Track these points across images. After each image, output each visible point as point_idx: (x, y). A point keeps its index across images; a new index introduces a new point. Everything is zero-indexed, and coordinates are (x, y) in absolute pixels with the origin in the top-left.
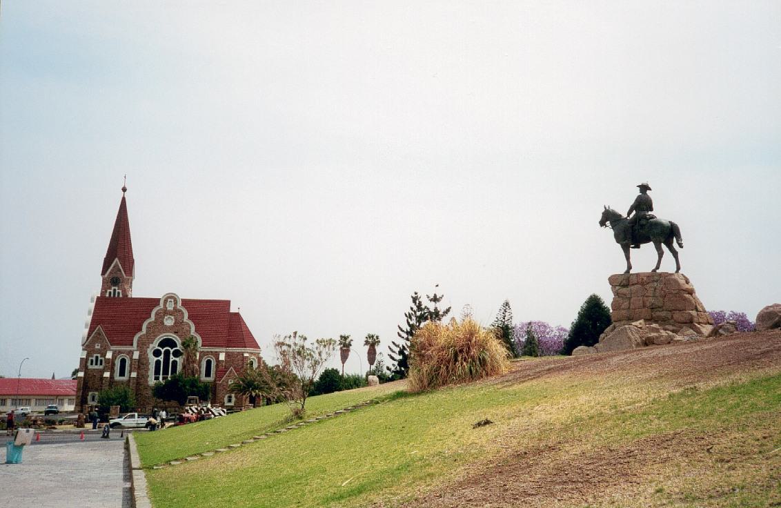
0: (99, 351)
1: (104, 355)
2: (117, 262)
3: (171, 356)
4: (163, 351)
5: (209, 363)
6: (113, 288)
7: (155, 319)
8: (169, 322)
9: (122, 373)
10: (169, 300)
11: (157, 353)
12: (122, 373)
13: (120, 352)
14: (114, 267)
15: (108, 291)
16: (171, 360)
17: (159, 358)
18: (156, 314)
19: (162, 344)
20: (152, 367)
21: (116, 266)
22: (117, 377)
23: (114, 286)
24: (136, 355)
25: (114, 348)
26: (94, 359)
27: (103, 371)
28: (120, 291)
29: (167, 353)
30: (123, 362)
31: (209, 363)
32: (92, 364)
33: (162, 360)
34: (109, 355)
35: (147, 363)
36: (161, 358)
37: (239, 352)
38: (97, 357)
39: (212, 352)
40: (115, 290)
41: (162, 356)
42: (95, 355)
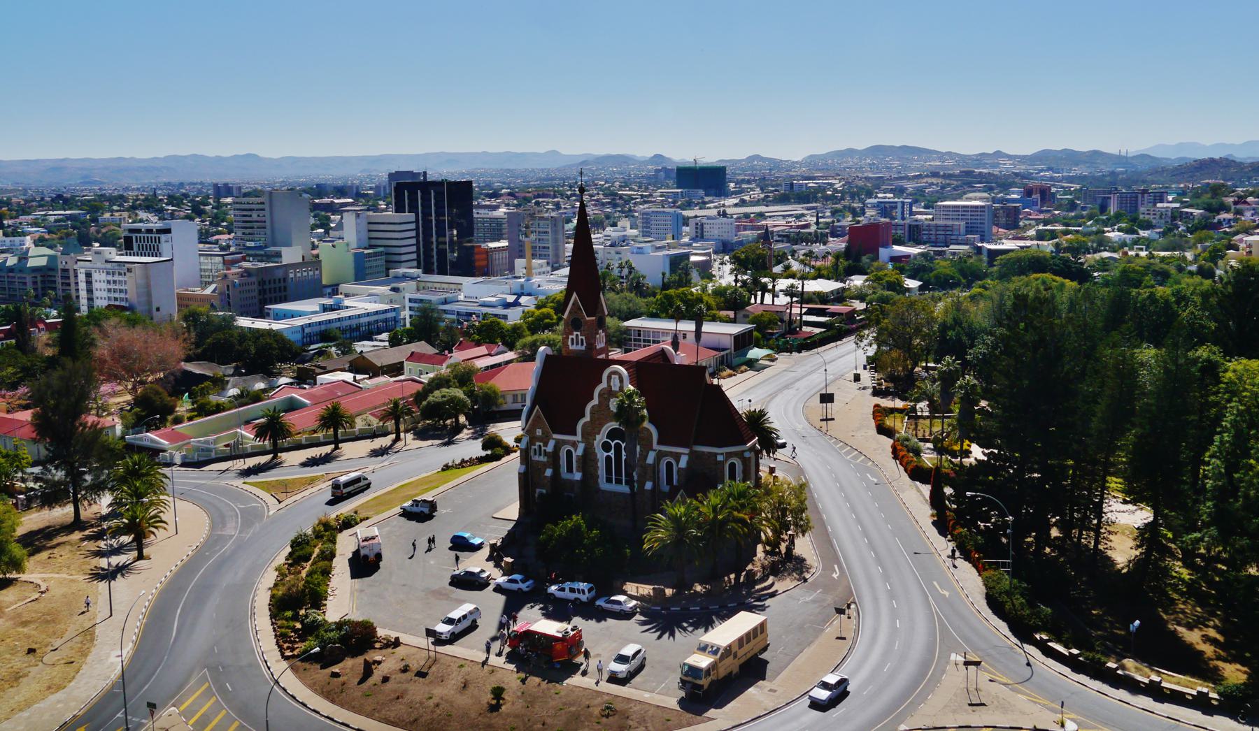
0: (540, 439)
1: (546, 445)
3: (624, 453)
4: (613, 444)
5: (669, 465)
6: (575, 333)
7: (599, 402)
8: (613, 405)
9: (570, 470)
10: (613, 376)
11: (606, 447)
12: (570, 470)
13: (565, 442)
14: (573, 304)
15: (570, 337)
16: (624, 458)
17: (609, 454)
18: (600, 395)
19: (613, 434)
20: (601, 465)
21: (575, 301)
22: (564, 473)
23: (576, 330)
24: (581, 447)
25: (555, 436)
26: (536, 447)
27: (545, 466)
28: (584, 338)
29: (618, 447)
30: (569, 453)
31: (669, 465)
32: (535, 454)
33: (613, 456)
34: (550, 448)
35: (596, 461)
36: (612, 453)
37: (709, 453)
38: (540, 446)
39: (671, 452)
40: (577, 335)
41: (613, 451)
42: (538, 444)
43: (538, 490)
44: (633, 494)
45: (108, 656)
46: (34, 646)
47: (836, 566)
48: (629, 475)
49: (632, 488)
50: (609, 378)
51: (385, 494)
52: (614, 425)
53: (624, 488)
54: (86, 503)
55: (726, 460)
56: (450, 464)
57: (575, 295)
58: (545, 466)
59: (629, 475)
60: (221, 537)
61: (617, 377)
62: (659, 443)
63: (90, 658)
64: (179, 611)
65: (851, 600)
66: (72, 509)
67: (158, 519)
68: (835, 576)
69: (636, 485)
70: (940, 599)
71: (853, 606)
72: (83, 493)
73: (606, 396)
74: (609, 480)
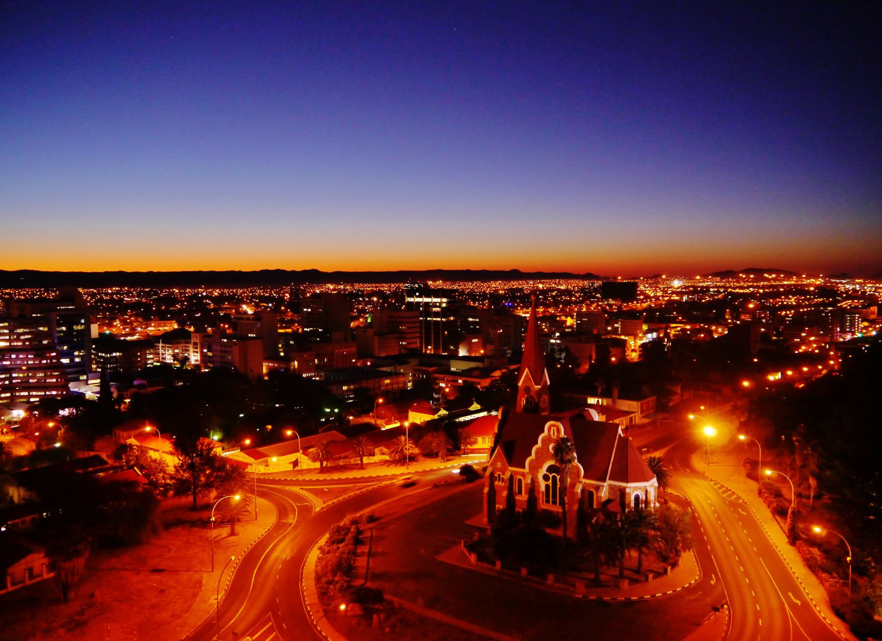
1: (503, 474)
2: (527, 372)
3: (558, 483)
4: (551, 476)
10: (552, 428)
12: (520, 492)
13: (516, 473)
14: (526, 376)
16: (558, 486)
17: (548, 483)
18: (543, 441)
19: (551, 469)
21: (527, 374)
25: (511, 468)
29: (554, 478)
34: (507, 475)
35: (539, 486)
36: (550, 482)
38: (499, 475)
41: (551, 481)
42: (498, 473)
43: (497, 506)
44: (564, 513)
45: (209, 598)
46: (164, 588)
47: (713, 576)
48: (562, 499)
49: (564, 508)
50: (549, 429)
51: (393, 502)
52: (552, 462)
53: (557, 509)
54: (201, 496)
55: (633, 492)
56: (438, 484)
57: (527, 370)
58: (502, 488)
59: (562, 499)
60: (285, 524)
61: (555, 428)
62: (585, 477)
63: (198, 599)
64: (255, 572)
65: (724, 601)
66: (192, 499)
67: (245, 509)
68: (712, 582)
69: (566, 506)
70: (793, 606)
71: (726, 606)
72: (199, 489)
73: (547, 442)
74: (548, 501)
